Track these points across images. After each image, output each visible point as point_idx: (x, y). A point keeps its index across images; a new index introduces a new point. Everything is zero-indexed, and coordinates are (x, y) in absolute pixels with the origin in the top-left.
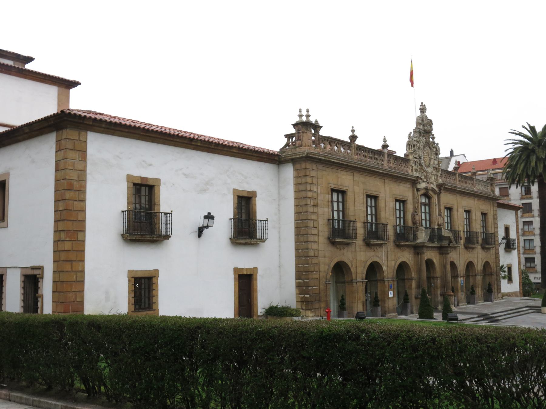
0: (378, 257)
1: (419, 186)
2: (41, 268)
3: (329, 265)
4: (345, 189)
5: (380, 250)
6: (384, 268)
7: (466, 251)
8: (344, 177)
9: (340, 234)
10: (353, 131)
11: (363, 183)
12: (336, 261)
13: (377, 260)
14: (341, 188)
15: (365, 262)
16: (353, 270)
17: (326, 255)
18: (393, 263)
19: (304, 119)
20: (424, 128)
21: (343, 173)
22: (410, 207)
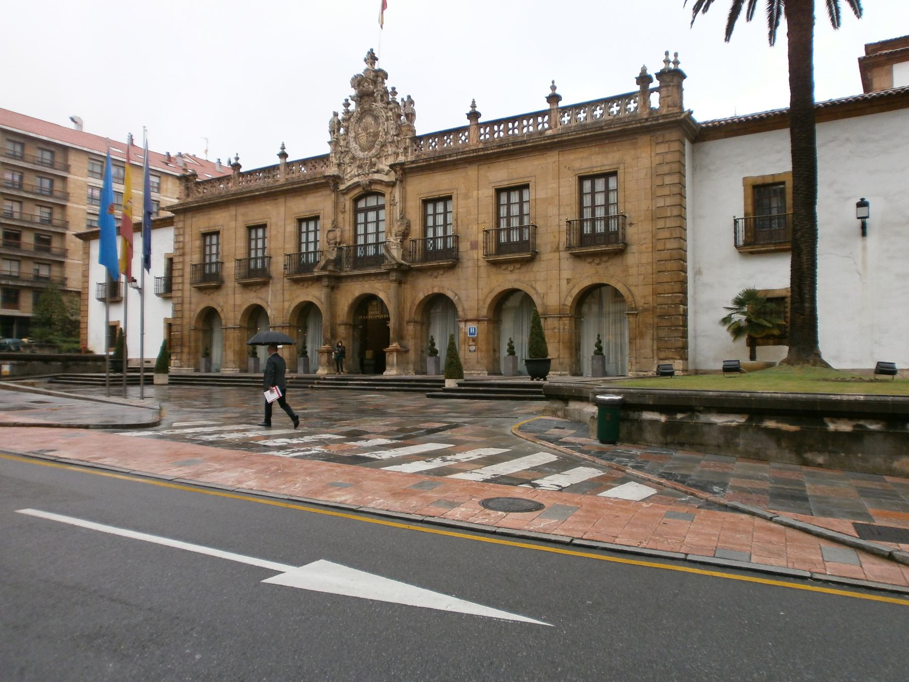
0: (261, 299)
1: (342, 187)
2: (119, 321)
3: (195, 311)
4: (217, 229)
5: (263, 290)
6: (269, 312)
7: (494, 270)
8: (218, 216)
9: (209, 279)
10: (553, 88)
11: (243, 215)
12: (202, 306)
13: (259, 302)
14: (212, 229)
15: (240, 306)
16: (222, 315)
17: (193, 300)
18: (287, 304)
19: (672, 66)
20: (370, 87)
21: (215, 212)
22: (326, 223)
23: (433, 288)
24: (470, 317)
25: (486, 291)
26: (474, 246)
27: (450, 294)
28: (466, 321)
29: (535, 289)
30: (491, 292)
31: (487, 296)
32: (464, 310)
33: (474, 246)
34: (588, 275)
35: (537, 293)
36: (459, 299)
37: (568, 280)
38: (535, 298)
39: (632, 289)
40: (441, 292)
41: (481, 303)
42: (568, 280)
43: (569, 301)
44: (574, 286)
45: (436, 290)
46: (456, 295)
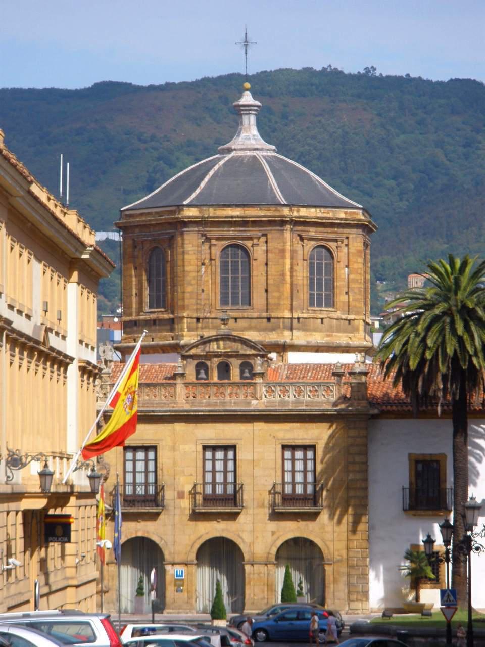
23: (136, 532)
24: (177, 560)
25: (193, 538)
26: (181, 495)
27: (155, 538)
28: (173, 564)
29: (242, 538)
30: (199, 538)
31: (195, 542)
32: (170, 554)
33: (181, 495)
34: (291, 529)
35: (244, 542)
36: (166, 543)
37: (273, 533)
38: (242, 547)
39: (328, 543)
40: (146, 535)
41: (189, 548)
42: (273, 533)
43: (274, 551)
44: (278, 538)
45: (140, 534)
46: (162, 539)
